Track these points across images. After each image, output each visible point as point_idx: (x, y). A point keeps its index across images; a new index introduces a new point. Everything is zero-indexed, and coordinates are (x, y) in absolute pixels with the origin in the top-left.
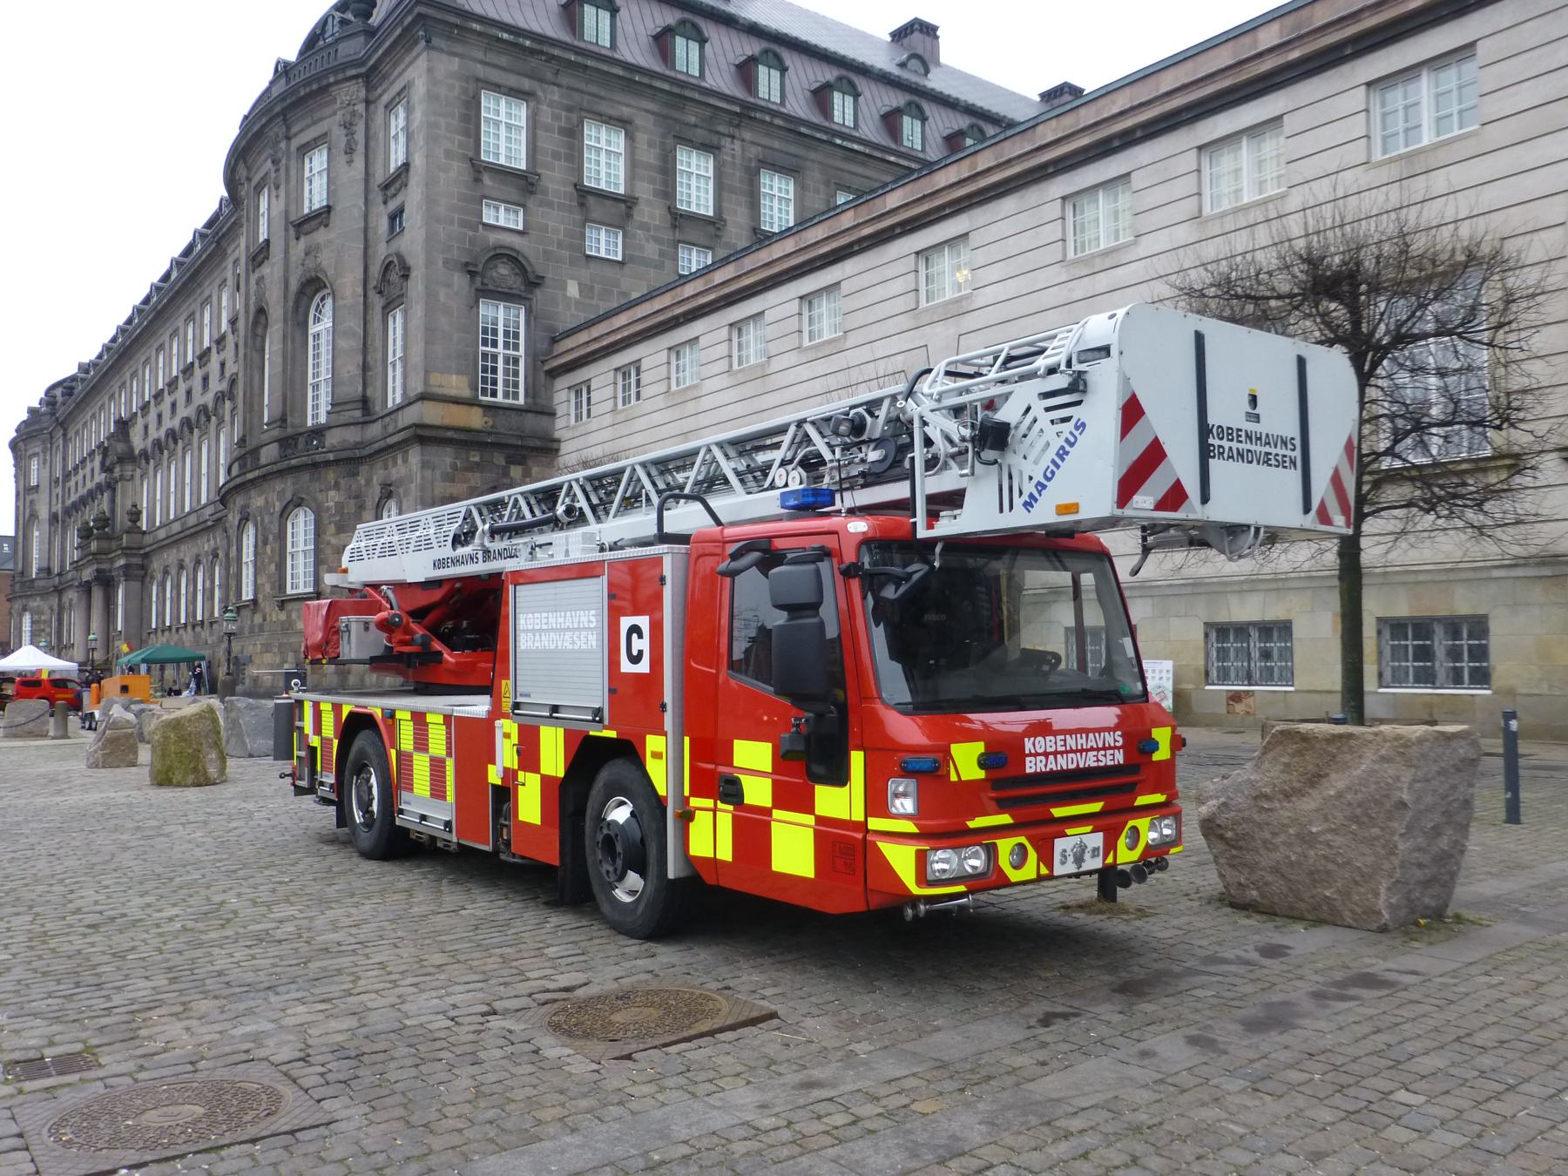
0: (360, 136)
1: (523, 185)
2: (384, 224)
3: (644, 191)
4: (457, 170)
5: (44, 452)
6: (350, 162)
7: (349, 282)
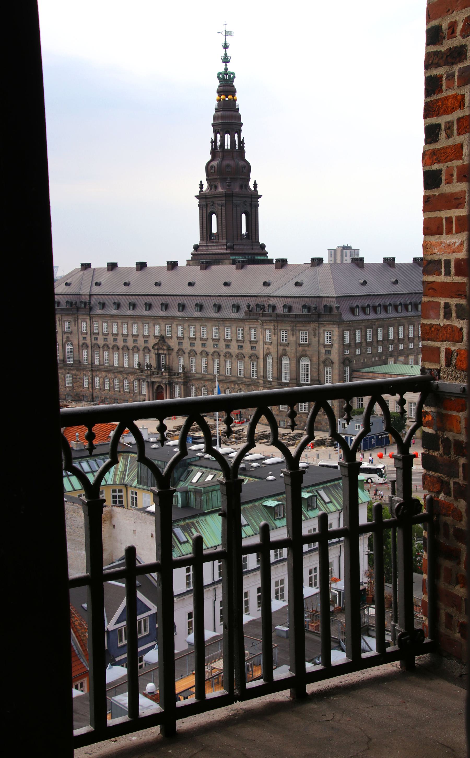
0: (317, 333)
1: (349, 346)
2: (323, 351)
3: (363, 341)
4: (342, 346)
5: (75, 321)
6: (315, 337)
7: (315, 359)
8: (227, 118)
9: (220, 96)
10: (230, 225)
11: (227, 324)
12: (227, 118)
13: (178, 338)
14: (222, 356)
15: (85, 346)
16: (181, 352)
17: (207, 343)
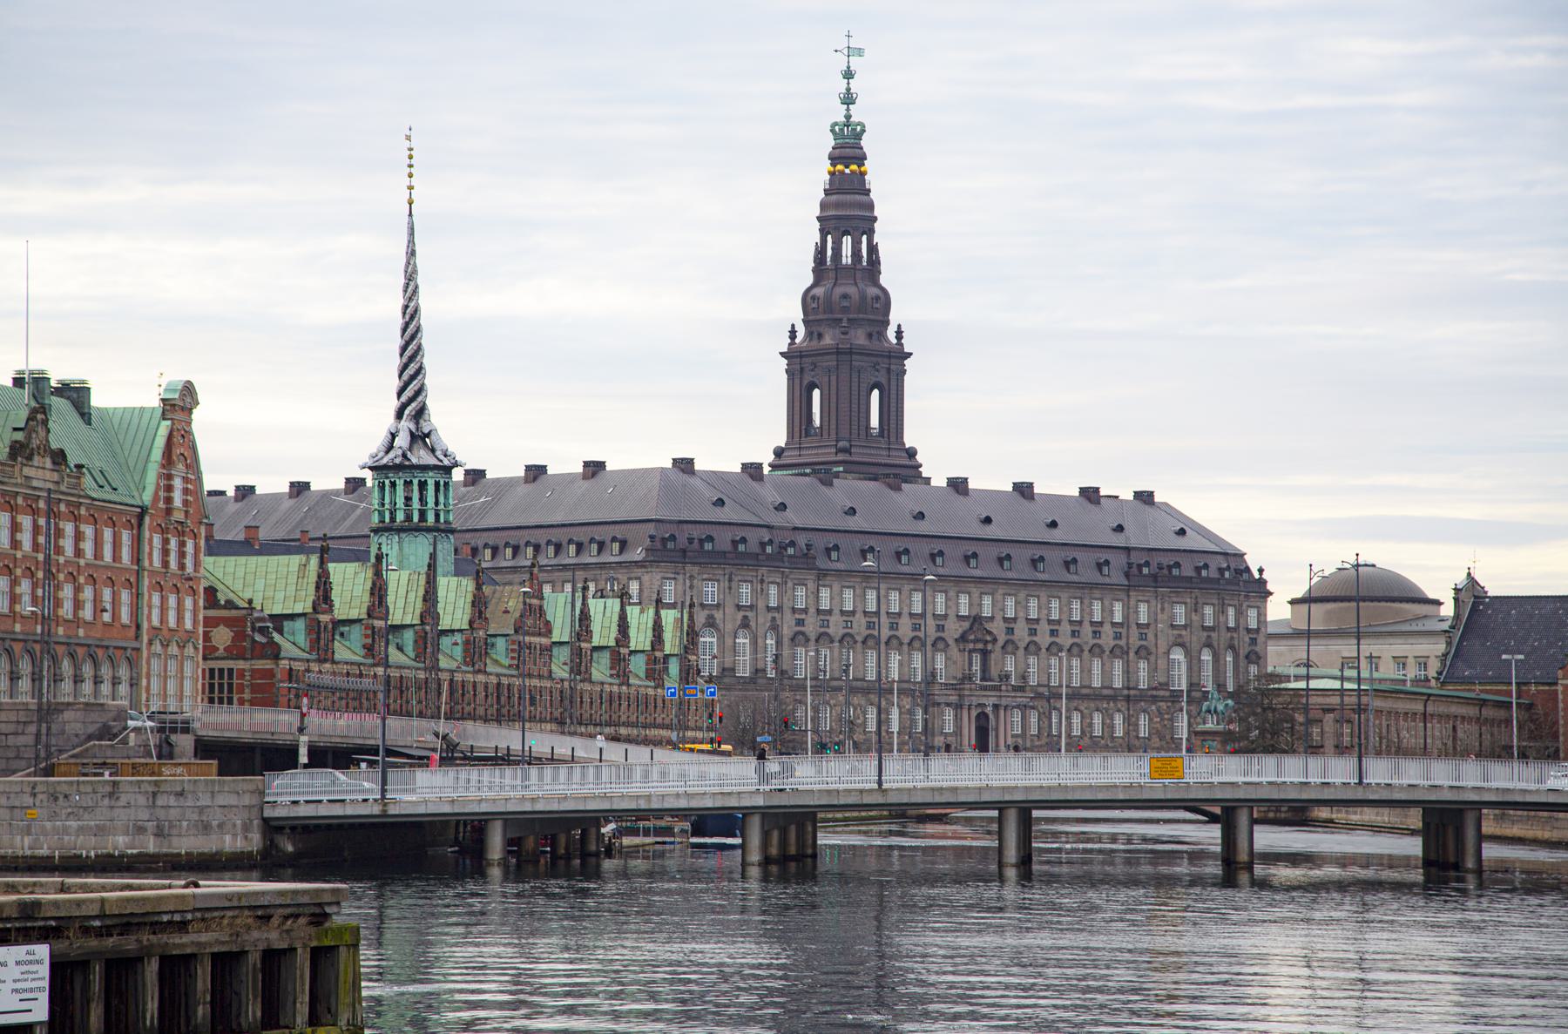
8: (847, 207)
9: (834, 165)
10: (847, 411)
11: (1097, 593)
12: (847, 207)
13: (1006, 620)
14: (1086, 653)
15: (799, 638)
16: (1010, 646)
17: (1060, 629)
